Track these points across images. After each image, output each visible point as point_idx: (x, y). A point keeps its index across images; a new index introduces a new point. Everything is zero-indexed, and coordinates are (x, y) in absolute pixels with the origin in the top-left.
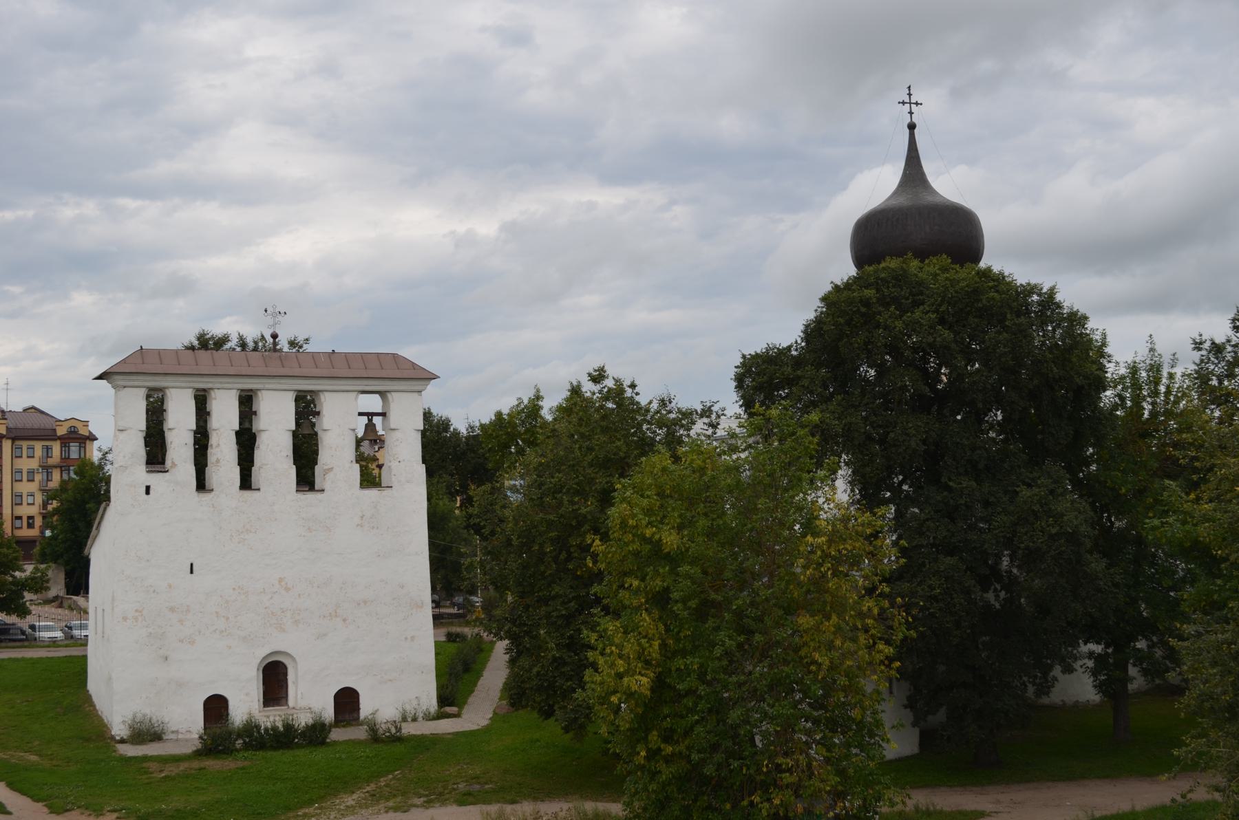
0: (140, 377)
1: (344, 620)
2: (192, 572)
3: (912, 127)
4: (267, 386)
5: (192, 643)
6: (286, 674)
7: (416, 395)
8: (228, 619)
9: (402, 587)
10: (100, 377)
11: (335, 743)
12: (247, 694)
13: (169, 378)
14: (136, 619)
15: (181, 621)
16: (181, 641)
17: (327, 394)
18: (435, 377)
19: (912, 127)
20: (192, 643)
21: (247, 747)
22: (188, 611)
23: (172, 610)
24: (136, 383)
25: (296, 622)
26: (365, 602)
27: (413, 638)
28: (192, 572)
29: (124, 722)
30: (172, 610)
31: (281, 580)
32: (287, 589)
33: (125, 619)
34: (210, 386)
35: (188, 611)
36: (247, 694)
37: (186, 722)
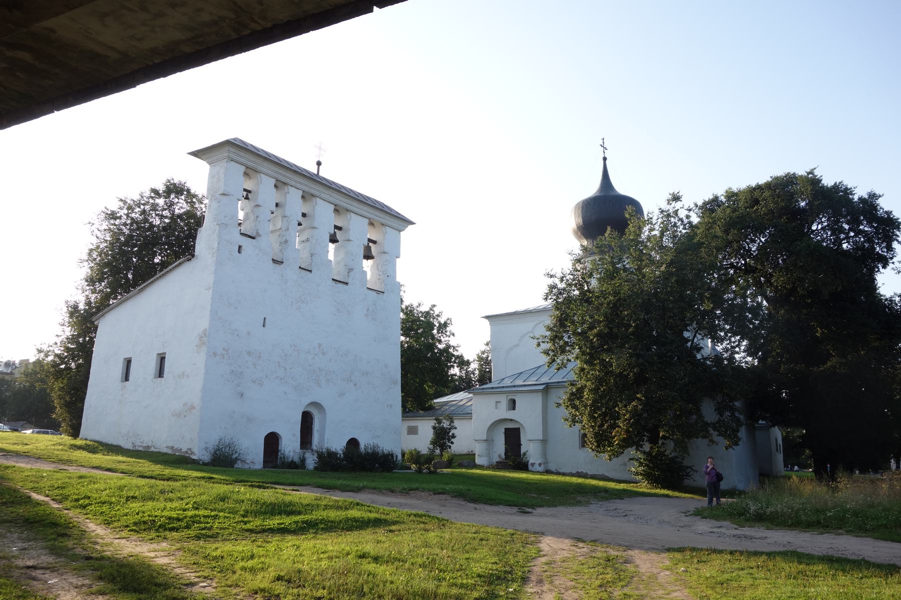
0: (248, 156)
3: (605, 159)
4: (323, 196)
5: (261, 385)
10: (196, 154)
13: (266, 164)
15: (254, 364)
16: (254, 382)
17: (352, 214)
19: (605, 159)
20: (261, 385)
22: (260, 357)
23: (249, 353)
24: (242, 160)
29: (206, 449)
30: (249, 353)
31: (320, 345)
32: (324, 354)
34: (288, 181)
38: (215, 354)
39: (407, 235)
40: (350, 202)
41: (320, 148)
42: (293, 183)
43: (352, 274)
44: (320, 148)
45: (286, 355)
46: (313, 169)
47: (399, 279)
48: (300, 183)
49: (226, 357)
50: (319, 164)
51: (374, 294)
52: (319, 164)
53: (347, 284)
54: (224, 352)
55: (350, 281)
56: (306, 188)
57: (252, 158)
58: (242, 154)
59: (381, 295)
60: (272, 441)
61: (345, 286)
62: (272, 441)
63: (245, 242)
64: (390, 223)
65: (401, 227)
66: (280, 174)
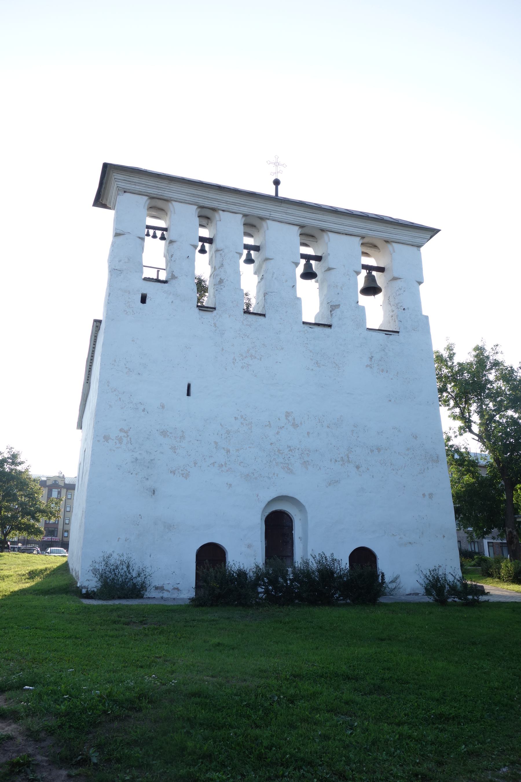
1: (358, 467)
2: (188, 394)
5: (186, 476)
6: (291, 528)
7: (415, 249)
8: (228, 451)
9: (416, 437)
11: (386, 605)
12: (249, 546)
13: (174, 187)
14: (120, 440)
15: (174, 449)
16: (173, 472)
17: (330, 234)
18: (434, 232)
20: (186, 476)
21: (272, 599)
22: (183, 437)
23: (164, 433)
25: (305, 464)
26: (379, 450)
27: (431, 495)
28: (188, 394)
31: (288, 415)
32: (295, 426)
33: (106, 438)
34: (214, 204)
35: (183, 437)
36: (249, 546)
37: (174, 575)
38: (106, 438)
39: (429, 250)
40: (320, 217)
41: (277, 164)
42: (223, 206)
43: (337, 312)
44: (277, 164)
45: (228, 432)
46: (271, 191)
47: (425, 312)
48: (234, 204)
49: (125, 440)
50: (277, 183)
51: (382, 335)
52: (277, 183)
53: (330, 326)
54: (122, 434)
55: (334, 322)
56: (246, 210)
57: (151, 182)
58: (136, 180)
59: (394, 336)
60: (211, 556)
61: (327, 330)
62: (211, 556)
63: (150, 289)
64: (398, 237)
65: (418, 241)
66: (199, 196)
